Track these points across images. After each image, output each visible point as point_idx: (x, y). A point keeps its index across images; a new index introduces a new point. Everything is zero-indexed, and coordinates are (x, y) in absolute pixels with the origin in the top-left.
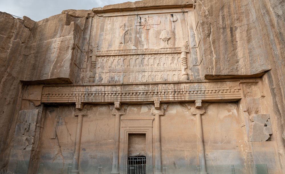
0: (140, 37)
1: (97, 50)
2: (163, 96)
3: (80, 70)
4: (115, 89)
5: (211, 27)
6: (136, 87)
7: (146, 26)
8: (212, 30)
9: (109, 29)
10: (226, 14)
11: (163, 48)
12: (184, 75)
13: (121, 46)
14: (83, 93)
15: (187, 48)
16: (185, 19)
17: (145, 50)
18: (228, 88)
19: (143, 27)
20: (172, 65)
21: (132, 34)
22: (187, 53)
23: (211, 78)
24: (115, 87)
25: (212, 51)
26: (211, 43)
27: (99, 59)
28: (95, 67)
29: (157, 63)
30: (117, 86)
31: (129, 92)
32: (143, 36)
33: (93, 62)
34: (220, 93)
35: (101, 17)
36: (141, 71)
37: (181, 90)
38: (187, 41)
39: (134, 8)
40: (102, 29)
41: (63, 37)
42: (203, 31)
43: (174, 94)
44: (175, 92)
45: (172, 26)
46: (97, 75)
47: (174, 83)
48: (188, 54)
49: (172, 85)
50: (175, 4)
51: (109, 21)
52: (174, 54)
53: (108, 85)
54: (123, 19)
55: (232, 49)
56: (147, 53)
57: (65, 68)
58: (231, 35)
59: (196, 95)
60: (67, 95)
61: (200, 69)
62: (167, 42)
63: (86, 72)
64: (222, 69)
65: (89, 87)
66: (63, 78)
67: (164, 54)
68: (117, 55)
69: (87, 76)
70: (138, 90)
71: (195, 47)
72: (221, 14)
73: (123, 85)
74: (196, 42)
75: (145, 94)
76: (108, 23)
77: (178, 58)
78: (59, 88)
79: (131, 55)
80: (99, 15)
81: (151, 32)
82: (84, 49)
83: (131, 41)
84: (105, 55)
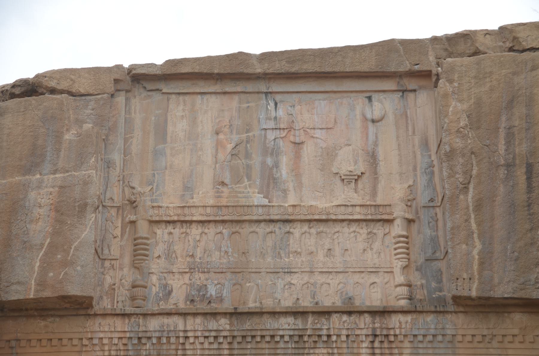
0: (277, 165)
1: (150, 203)
2: (344, 345)
3: (103, 265)
4: (213, 325)
5: (474, 162)
6: (270, 320)
7: (292, 132)
8: (474, 172)
10: (517, 123)
11: (344, 203)
12: (400, 285)
13: (222, 192)
14: (122, 335)
15: (410, 206)
16: (406, 112)
17: (290, 210)
18: (516, 331)
19: (283, 134)
20: (369, 255)
21: (253, 155)
22: (410, 221)
23: (470, 302)
24: (215, 318)
25: (473, 233)
26: (471, 208)
27: (159, 232)
28: (147, 256)
29: (326, 247)
30: (218, 317)
31: (253, 333)
32: (284, 160)
33: (140, 241)
34: (495, 344)
35: (153, 93)
36: (281, 270)
37: (392, 332)
38: (411, 183)
39: (259, 73)
40: (161, 133)
41: (64, 173)
42: (450, 176)
43: (372, 342)
44: (376, 336)
45: (367, 134)
46: (154, 279)
47: (374, 313)
48: (412, 223)
49: (367, 318)
51: (181, 107)
52: (372, 224)
53: (195, 315)
54: (223, 105)
55: (527, 226)
56: (298, 217)
57: (79, 268)
58: (528, 187)
59: (430, 345)
60: (75, 342)
61: (444, 270)
62: (353, 184)
63: (121, 269)
64: (496, 280)
65: (141, 317)
66: (76, 296)
67: (345, 224)
68: (209, 221)
69: (123, 281)
70: (276, 327)
71: (431, 204)
72: (503, 124)
73: (235, 314)
74: (435, 189)
75: (296, 339)
76: (178, 114)
77: (385, 235)
78: (49, 320)
79: (251, 221)
80: (150, 86)
81: (309, 151)
82: (112, 199)
83: (249, 178)
84: (176, 218)
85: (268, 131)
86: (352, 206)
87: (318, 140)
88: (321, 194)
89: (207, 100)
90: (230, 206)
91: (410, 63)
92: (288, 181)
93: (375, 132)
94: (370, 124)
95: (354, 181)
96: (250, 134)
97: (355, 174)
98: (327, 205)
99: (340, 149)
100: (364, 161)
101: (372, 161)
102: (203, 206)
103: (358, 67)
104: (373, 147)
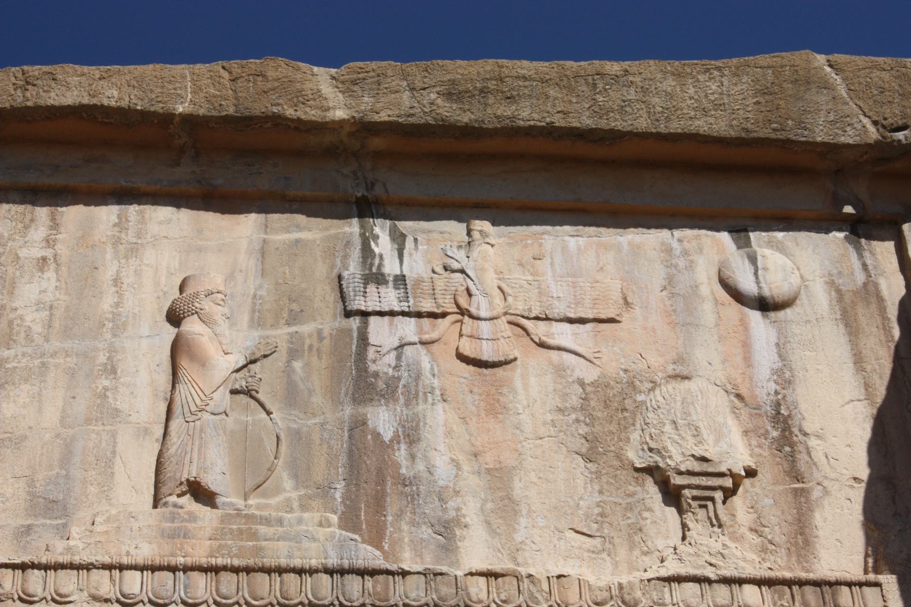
0: (411, 434)
9: (34, 319)
11: (693, 572)
16: (876, 285)
32: (437, 418)
39: (342, 122)
45: (746, 346)
50: (765, 132)
51: (39, 233)
54: (200, 231)
76: (23, 253)
81: (533, 387)
83: (300, 475)
85: (373, 320)
86: (727, 581)
87: (565, 355)
88: (597, 542)
89: (141, 213)
90: (225, 568)
91: (875, 123)
92: (457, 493)
93: (773, 339)
94: (755, 316)
95: (719, 496)
96: (306, 329)
97: (723, 469)
98: (624, 581)
99: (652, 389)
100: (746, 433)
101: (775, 434)
102: (109, 567)
103: (697, 123)
104: (772, 387)
